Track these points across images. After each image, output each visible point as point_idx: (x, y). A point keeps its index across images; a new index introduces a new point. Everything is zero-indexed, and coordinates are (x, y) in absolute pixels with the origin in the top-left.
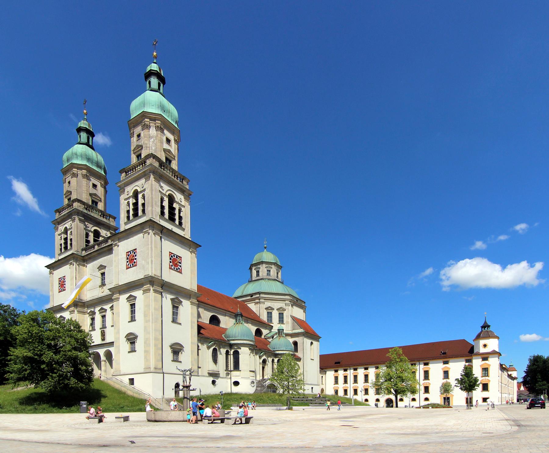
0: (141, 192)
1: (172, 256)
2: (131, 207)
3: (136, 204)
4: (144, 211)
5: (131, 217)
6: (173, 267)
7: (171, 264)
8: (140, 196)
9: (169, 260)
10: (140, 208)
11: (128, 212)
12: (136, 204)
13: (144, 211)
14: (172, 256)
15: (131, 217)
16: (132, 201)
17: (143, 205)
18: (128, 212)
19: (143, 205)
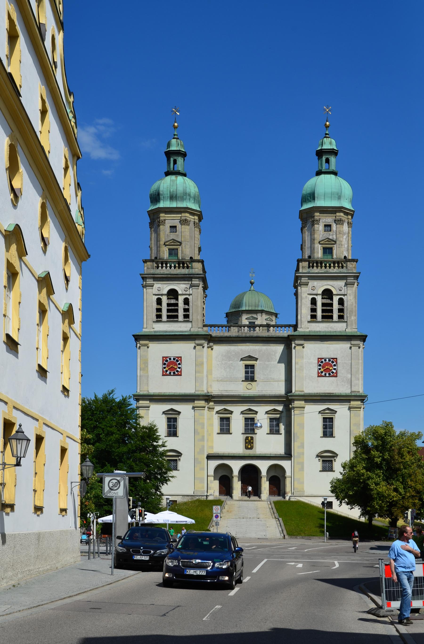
5: (164, 318)
11: (159, 310)
13: (186, 316)
15: (164, 318)
18: (159, 310)
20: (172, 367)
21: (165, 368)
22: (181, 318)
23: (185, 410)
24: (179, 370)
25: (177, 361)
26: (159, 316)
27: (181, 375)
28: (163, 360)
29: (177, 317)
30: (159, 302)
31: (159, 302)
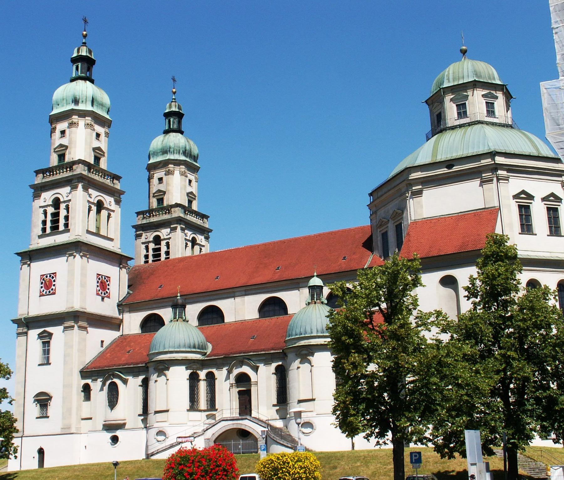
0: (64, 202)
1: (99, 279)
2: (49, 218)
3: (56, 215)
4: (66, 225)
5: (48, 231)
6: (100, 292)
7: (99, 288)
8: (63, 206)
9: (96, 284)
10: (62, 221)
11: (44, 222)
12: (56, 215)
13: (66, 225)
14: (99, 279)
15: (48, 231)
16: (51, 210)
17: (67, 218)
18: (44, 222)
19: (67, 218)
20: (48, 284)
21: (42, 287)
22: (62, 228)
23: (56, 331)
24: (53, 287)
25: (53, 278)
26: (44, 230)
27: (54, 294)
28: (41, 278)
29: (57, 227)
30: (45, 213)
31: (45, 213)
